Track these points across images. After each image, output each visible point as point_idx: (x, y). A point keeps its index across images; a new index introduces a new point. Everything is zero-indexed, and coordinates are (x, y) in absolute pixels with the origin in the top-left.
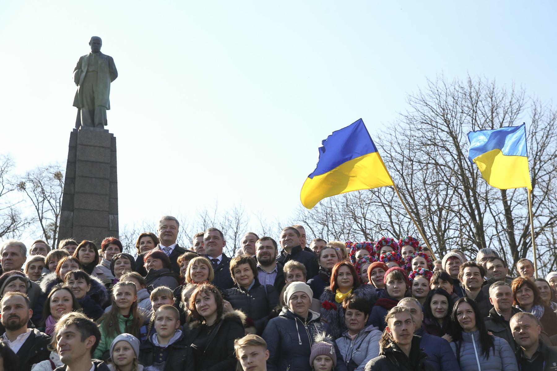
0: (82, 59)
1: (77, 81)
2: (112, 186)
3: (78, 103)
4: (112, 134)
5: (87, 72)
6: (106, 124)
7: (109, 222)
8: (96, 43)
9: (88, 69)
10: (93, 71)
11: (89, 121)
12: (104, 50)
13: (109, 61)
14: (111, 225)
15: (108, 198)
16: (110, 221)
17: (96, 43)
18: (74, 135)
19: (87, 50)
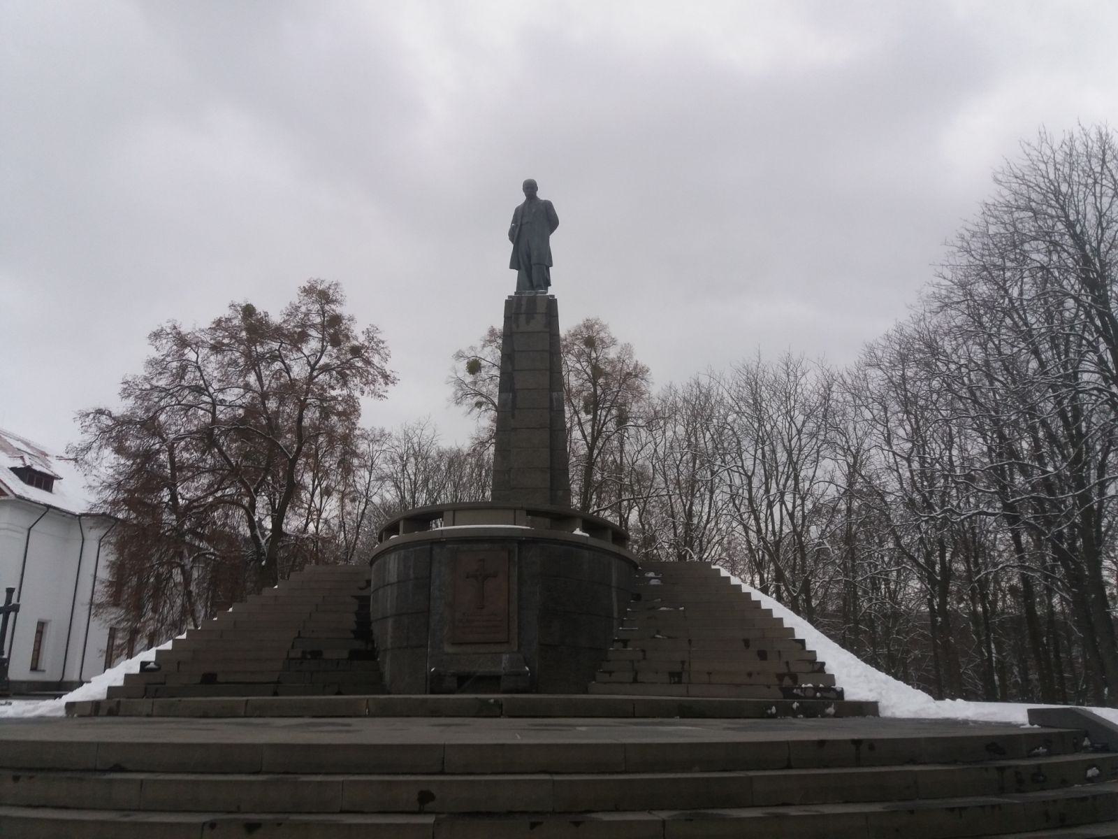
0: (517, 210)
1: (512, 239)
2: (555, 359)
3: (515, 264)
4: (553, 296)
5: (521, 225)
6: (548, 283)
7: (551, 400)
8: (530, 188)
9: (521, 222)
10: (527, 223)
11: (528, 284)
12: (542, 195)
13: (548, 207)
14: (555, 403)
15: (548, 373)
16: (554, 400)
17: (530, 188)
18: (509, 304)
19: (521, 198)
